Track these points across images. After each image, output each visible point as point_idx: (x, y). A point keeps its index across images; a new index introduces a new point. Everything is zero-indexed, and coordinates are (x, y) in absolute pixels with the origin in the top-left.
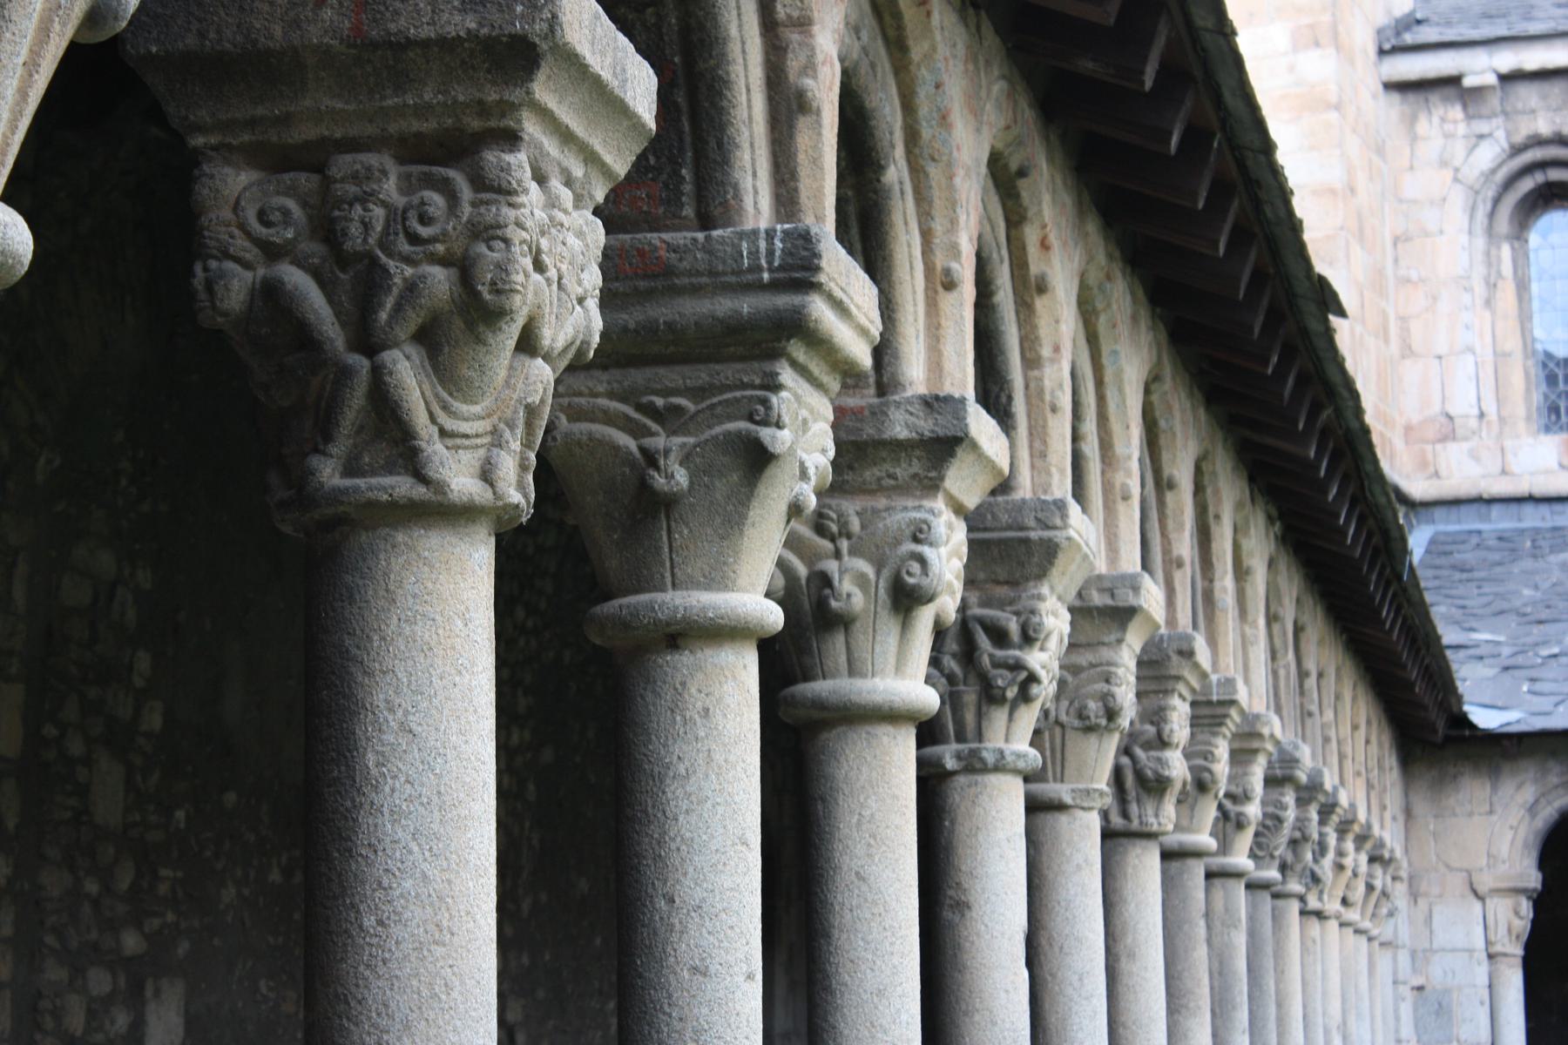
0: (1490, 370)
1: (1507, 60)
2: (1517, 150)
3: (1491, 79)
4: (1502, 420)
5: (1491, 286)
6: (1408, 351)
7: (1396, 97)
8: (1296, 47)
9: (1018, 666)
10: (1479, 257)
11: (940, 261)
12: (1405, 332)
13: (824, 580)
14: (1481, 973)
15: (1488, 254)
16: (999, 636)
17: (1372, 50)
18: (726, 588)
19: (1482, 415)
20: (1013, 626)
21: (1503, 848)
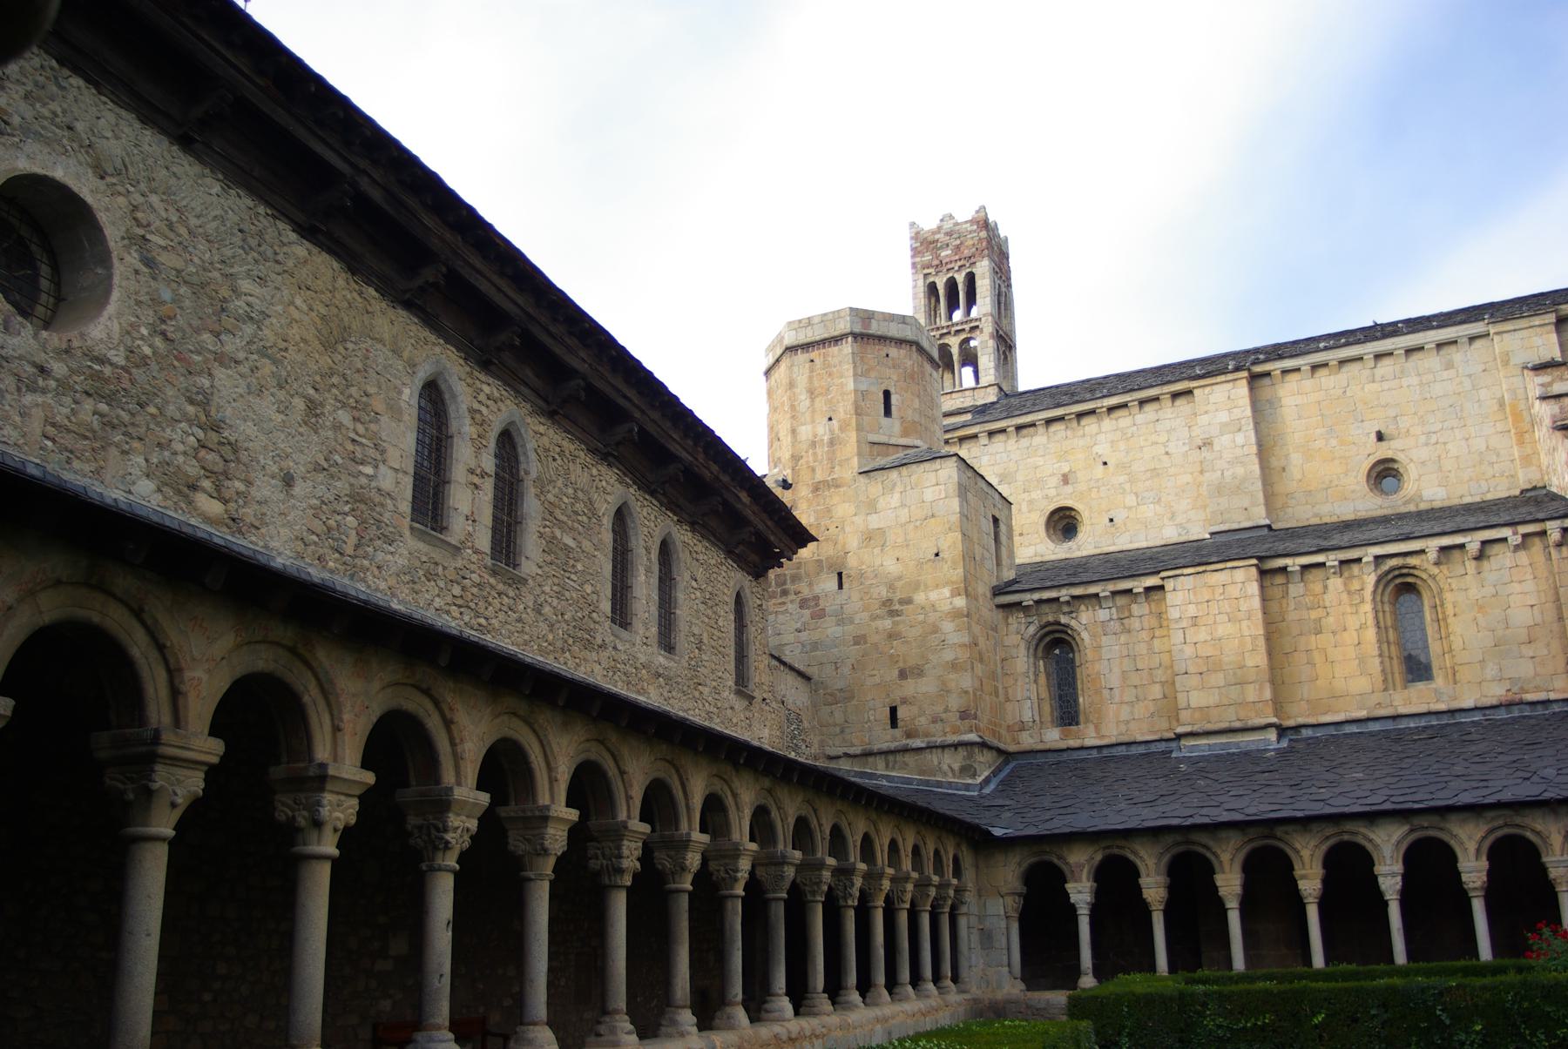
0: (1036, 705)
1: (1036, 596)
2: (1043, 627)
3: (1031, 603)
4: (1041, 722)
5: (1036, 675)
6: (1008, 700)
7: (1001, 610)
8: (953, 596)
9: (442, 838)
10: (1031, 665)
11: (336, 722)
12: (1006, 693)
13: (294, 817)
14: (1003, 924)
15: (1035, 664)
16: (438, 830)
17: (989, 594)
18: (147, 826)
19: (1034, 721)
20: (441, 826)
21: (1010, 878)
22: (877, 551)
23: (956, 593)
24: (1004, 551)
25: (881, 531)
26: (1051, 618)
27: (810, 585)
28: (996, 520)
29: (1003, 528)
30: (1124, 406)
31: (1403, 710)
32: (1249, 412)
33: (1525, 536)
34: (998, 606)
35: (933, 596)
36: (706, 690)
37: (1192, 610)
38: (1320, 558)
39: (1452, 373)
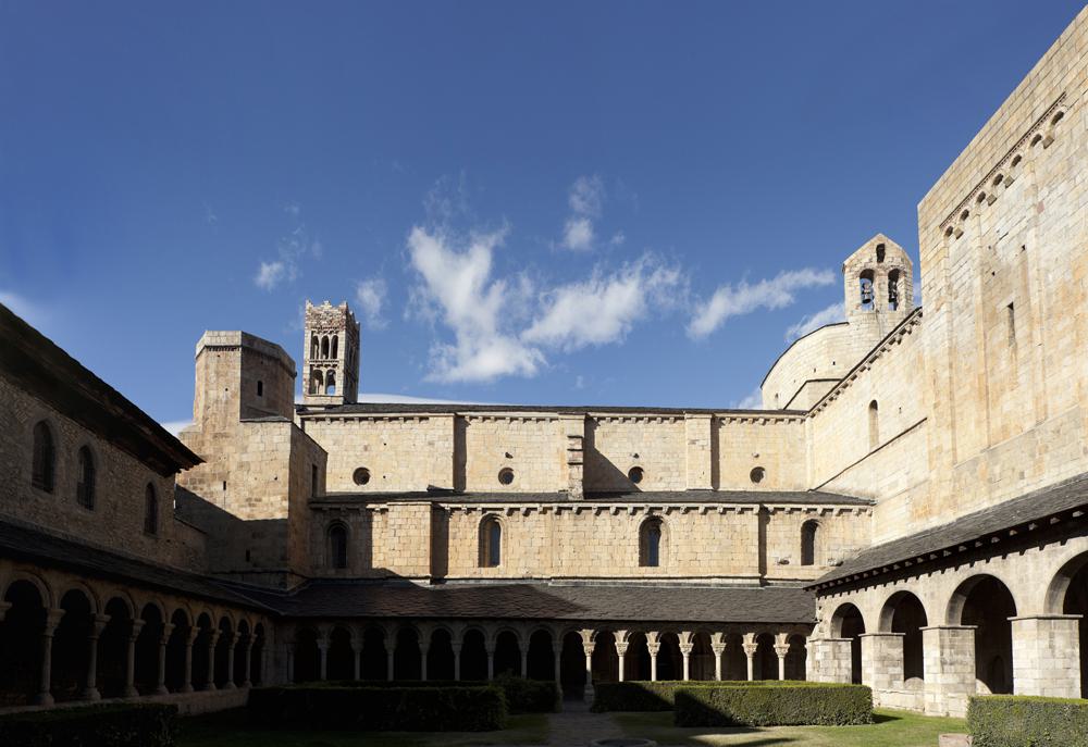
17: (305, 502)
22: (245, 473)
23: (284, 499)
24: (319, 484)
25: (248, 463)
26: (336, 518)
27: (209, 486)
28: (315, 468)
29: (319, 471)
30: (397, 419)
31: (484, 576)
32: (452, 433)
33: (544, 508)
34: (311, 509)
35: (272, 499)
36: (119, 532)
37: (399, 522)
38: (459, 506)
39: (540, 433)
